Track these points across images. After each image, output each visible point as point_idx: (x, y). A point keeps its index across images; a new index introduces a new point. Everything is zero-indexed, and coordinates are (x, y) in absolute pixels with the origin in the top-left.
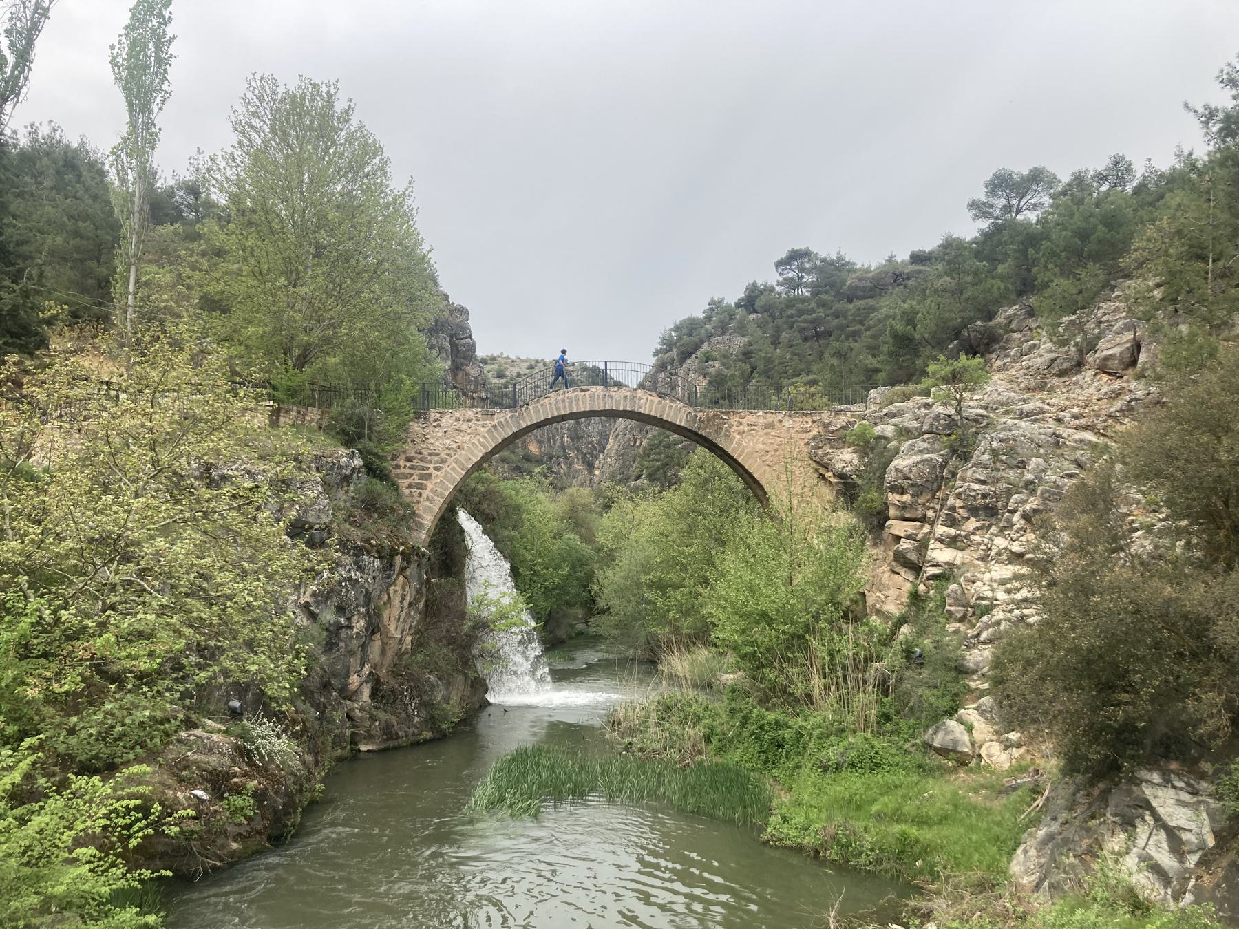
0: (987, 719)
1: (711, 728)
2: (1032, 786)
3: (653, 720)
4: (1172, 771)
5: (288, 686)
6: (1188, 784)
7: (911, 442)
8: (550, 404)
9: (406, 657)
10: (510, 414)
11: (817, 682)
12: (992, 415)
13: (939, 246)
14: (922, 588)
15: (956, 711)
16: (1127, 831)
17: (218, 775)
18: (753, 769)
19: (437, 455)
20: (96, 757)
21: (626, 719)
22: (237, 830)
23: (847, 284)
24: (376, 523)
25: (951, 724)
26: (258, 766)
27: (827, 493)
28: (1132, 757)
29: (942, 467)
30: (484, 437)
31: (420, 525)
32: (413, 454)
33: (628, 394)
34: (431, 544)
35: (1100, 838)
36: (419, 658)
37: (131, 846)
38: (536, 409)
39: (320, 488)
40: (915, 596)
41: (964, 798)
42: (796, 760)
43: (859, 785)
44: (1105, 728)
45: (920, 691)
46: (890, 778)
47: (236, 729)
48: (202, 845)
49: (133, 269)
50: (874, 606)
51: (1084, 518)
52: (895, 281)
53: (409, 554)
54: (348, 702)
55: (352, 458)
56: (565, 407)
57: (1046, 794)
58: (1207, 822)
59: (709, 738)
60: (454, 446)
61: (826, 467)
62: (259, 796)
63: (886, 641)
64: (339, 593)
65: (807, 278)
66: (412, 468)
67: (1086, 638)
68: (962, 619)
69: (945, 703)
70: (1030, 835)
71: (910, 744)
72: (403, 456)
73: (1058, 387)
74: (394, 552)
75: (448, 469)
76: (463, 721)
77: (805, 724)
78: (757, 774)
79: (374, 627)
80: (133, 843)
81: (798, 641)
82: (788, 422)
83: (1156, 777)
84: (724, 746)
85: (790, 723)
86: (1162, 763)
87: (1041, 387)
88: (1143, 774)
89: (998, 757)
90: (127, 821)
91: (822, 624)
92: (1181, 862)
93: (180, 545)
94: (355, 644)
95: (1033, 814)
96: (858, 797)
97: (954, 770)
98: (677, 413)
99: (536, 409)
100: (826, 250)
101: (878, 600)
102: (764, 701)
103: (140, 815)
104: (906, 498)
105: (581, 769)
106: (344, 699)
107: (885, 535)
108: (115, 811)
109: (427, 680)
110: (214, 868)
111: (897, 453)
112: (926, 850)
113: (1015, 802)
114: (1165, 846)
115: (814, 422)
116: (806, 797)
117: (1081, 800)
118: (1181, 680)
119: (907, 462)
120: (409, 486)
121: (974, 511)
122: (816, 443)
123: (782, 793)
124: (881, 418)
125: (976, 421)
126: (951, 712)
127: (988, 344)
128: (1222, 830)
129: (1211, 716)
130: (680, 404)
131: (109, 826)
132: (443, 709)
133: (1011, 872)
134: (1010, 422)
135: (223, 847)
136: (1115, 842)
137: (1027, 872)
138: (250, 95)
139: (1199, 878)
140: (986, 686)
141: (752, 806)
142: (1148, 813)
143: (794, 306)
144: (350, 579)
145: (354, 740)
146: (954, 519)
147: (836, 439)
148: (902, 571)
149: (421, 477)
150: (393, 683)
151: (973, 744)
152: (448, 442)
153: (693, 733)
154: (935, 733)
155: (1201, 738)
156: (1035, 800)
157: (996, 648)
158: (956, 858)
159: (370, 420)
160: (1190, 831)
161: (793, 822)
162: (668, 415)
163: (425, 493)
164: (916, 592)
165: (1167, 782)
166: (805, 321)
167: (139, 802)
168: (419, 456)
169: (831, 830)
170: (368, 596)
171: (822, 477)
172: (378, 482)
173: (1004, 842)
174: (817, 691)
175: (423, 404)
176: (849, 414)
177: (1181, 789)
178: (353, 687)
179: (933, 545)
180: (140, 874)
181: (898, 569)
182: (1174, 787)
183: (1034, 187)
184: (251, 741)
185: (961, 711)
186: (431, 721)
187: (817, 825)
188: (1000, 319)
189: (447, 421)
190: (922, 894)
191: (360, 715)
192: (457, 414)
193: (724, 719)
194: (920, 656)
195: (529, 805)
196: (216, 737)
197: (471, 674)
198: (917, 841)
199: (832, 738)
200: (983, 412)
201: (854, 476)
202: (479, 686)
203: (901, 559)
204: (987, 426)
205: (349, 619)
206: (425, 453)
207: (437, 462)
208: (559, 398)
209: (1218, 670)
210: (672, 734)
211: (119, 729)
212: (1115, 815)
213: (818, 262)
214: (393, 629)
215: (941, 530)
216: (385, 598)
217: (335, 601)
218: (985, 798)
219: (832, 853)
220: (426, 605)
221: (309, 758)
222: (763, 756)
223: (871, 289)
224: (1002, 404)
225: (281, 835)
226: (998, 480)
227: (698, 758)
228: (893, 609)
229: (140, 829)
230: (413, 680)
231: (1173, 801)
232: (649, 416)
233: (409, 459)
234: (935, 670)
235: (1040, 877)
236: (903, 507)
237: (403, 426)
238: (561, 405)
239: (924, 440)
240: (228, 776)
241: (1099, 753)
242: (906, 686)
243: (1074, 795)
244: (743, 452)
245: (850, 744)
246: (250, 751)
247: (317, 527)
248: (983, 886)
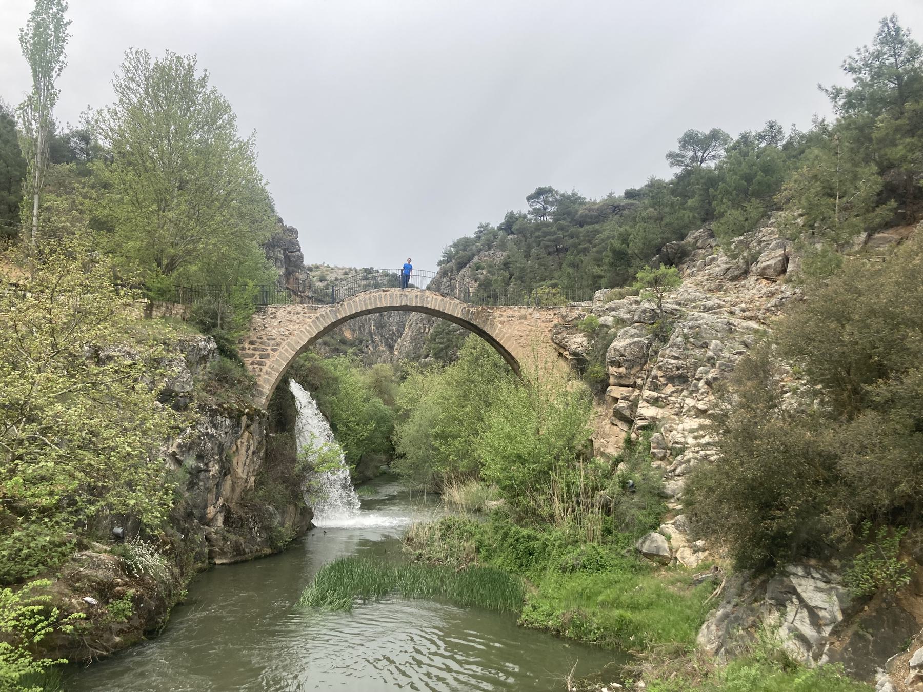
0: (680, 531)
1: (480, 542)
2: (713, 579)
3: (437, 537)
4: (811, 566)
5: (159, 515)
6: (823, 576)
7: (625, 329)
8: (360, 301)
9: (251, 492)
10: (329, 309)
11: (558, 506)
13: (646, 186)
14: (633, 436)
15: (659, 526)
16: (779, 610)
17: (104, 585)
18: (511, 571)
19: (274, 339)
20: (8, 573)
21: (417, 535)
22: (120, 627)
23: (580, 213)
24: (227, 391)
25: (655, 535)
26: (136, 577)
28: (783, 557)
29: (648, 347)
30: (310, 326)
31: (261, 393)
32: (255, 339)
33: (419, 293)
35: (761, 616)
36: (261, 493)
37: (35, 641)
39: (184, 365)
40: (629, 442)
41: (665, 589)
42: (543, 564)
43: (589, 581)
44: (764, 535)
45: (633, 511)
46: (613, 576)
47: (119, 549)
48: (92, 640)
50: (599, 449)
51: (749, 383)
52: (614, 211)
53: (252, 415)
54: (206, 527)
55: (208, 342)
56: (371, 304)
57: (723, 585)
58: (837, 603)
59: (479, 549)
60: (287, 332)
62: (137, 600)
63: (608, 475)
64: (199, 445)
65: (551, 209)
66: (254, 349)
67: (750, 470)
68: (663, 459)
69: (651, 520)
70: (712, 615)
71: (625, 551)
72: (248, 341)
73: (731, 289)
74: (241, 414)
75: (282, 350)
76: (295, 540)
77: (549, 537)
78: (514, 575)
79: (226, 470)
80: (37, 638)
81: (543, 475)
82: (537, 315)
83: (800, 571)
84: (490, 554)
85: (539, 536)
86: (804, 561)
87: (719, 289)
88: (791, 568)
89: (689, 558)
90: (32, 621)
91: (561, 463)
92: (819, 632)
93: (74, 409)
94: (211, 483)
95: (713, 600)
96: (588, 590)
97: (657, 569)
98: (455, 308)
100: (563, 188)
102: (519, 520)
103: (43, 618)
105: (384, 574)
106: (203, 525)
107: (607, 398)
108: (23, 614)
109: (267, 510)
110: (102, 657)
111: (616, 337)
112: (638, 628)
113: (701, 591)
114: (807, 621)
116: (550, 591)
117: (747, 589)
118: (817, 500)
120: (252, 364)
121: (670, 379)
122: (557, 332)
123: (533, 589)
124: (604, 311)
125: (672, 313)
126: (655, 527)
127: (680, 258)
128: (848, 608)
129: (839, 526)
130: (457, 301)
131: (18, 626)
132: (280, 532)
133: (698, 642)
134: (697, 314)
135: (108, 640)
136: (772, 619)
137: (709, 642)
138: (127, 64)
139: (832, 644)
140: (680, 507)
141: (510, 599)
142: (794, 597)
143: (540, 229)
144: (207, 434)
145: (211, 555)
146: (657, 385)
147: (571, 327)
148: (619, 423)
149: (261, 357)
150: (240, 512)
151: (671, 550)
152: (282, 329)
153: (468, 545)
154: (644, 542)
155: (832, 542)
156: (715, 589)
157: (687, 479)
158: (659, 634)
159: (222, 313)
160: (825, 609)
161: (541, 609)
162: (448, 309)
163: (265, 369)
164: (630, 439)
165: (808, 574)
166: (549, 241)
167: (41, 607)
168: (260, 341)
169: (568, 616)
170: (221, 448)
172: (229, 360)
173: (693, 620)
174: (558, 512)
175: (262, 301)
176: (580, 308)
177: (818, 579)
178: (210, 516)
179: (641, 404)
180: (43, 663)
182: (813, 578)
183: (714, 144)
184: (131, 558)
185: (662, 526)
186: (270, 541)
187: (558, 612)
188: (690, 239)
189: (281, 313)
190: (634, 660)
191: (215, 536)
192: (289, 309)
193: (490, 534)
194: (633, 486)
195: (345, 602)
196: (103, 556)
197: (301, 505)
198: (631, 622)
199: (569, 547)
200: (677, 307)
201: (584, 354)
202: (307, 513)
203: (618, 415)
204: (680, 317)
205: (206, 464)
206: (265, 338)
208: (367, 297)
209: (843, 492)
210: (451, 546)
211: (25, 551)
212: (772, 599)
213: (558, 197)
214: (241, 472)
215: (647, 393)
216: (234, 448)
217: (196, 450)
218: (680, 589)
219: (569, 633)
220: (266, 453)
221: (176, 570)
222: (519, 562)
223: (597, 217)
224: (690, 301)
225: (154, 630)
226: (688, 357)
227: (471, 564)
228: (613, 451)
229: (43, 628)
230: (256, 510)
231: (812, 588)
232: (434, 310)
233: (252, 343)
234: (643, 496)
235: (718, 645)
236: (620, 376)
237: (248, 318)
238: (368, 302)
239: (635, 328)
240: (112, 586)
241: (759, 554)
242: (622, 507)
243: (742, 585)
244: (503, 336)
245: (582, 551)
246: (129, 566)
247: (181, 394)
248: (678, 653)
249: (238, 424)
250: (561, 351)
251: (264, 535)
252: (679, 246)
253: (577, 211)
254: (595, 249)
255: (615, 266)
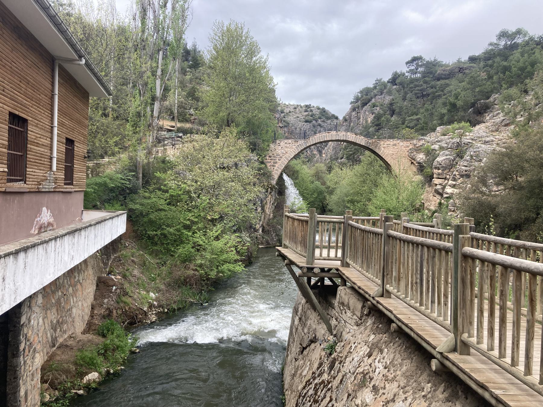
7: (444, 151)
10: (303, 141)
12: (474, 142)
13: (482, 53)
14: (443, 201)
27: (415, 169)
29: (453, 161)
30: (295, 149)
31: (274, 179)
32: (271, 155)
34: (277, 184)
36: (275, 220)
38: (312, 139)
40: (440, 204)
49: (176, 91)
52: (459, 71)
56: (322, 139)
60: (285, 152)
61: (414, 159)
65: (420, 69)
66: (271, 160)
68: (454, 211)
72: (268, 156)
73: (503, 131)
82: (401, 144)
87: (497, 130)
98: (362, 140)
99: (312, 139)
100: (428, 57)
101: (428, 205)
104: (440, 171)
107: (432, 184)
111: (439, 155)
115: (411, 143)
119: (440, 159)
121: (462, 176)
122: (411, 151)
124: (435, 142)
125: (467, 144)
127: (485, 109)
130: (363, 137)
134: (479, 145)
138: (214, 27)
143: (413, 82)
146: (455, 178)
147: (418, 150)
148: (437, 196)
150: (268, 228)
152: (283, 151)
163: (275, 168)
164: (441, 202)
166: (418, 90)
171: (412, 163)
181: (436, 195)
183: (518, 36)
188: (491, 99)
189: (282, 144)
192: (286, 141)
200: (470, 141)
203: (437, 192)
205: (256, 208)
206: (275, 154)
207: (279, 158)
214: (267, 211)
215: (450, 182)
216: (265, 202)
223: (448, 75)
224: (479, 138)
226: (471, 166)
228: (433, 208)
232: (351, 142)
233: (270, 157)
236: (439, 174)
237: (268, 146)
238: (321, 138)
239: (448, 151)
244: (385, 154)
249: (267, 192)
250: (413, 161)
251: (277, 238)
252: (485, 103)
253: (436, 72)
254: (444, 97)
255: (451, 112)
